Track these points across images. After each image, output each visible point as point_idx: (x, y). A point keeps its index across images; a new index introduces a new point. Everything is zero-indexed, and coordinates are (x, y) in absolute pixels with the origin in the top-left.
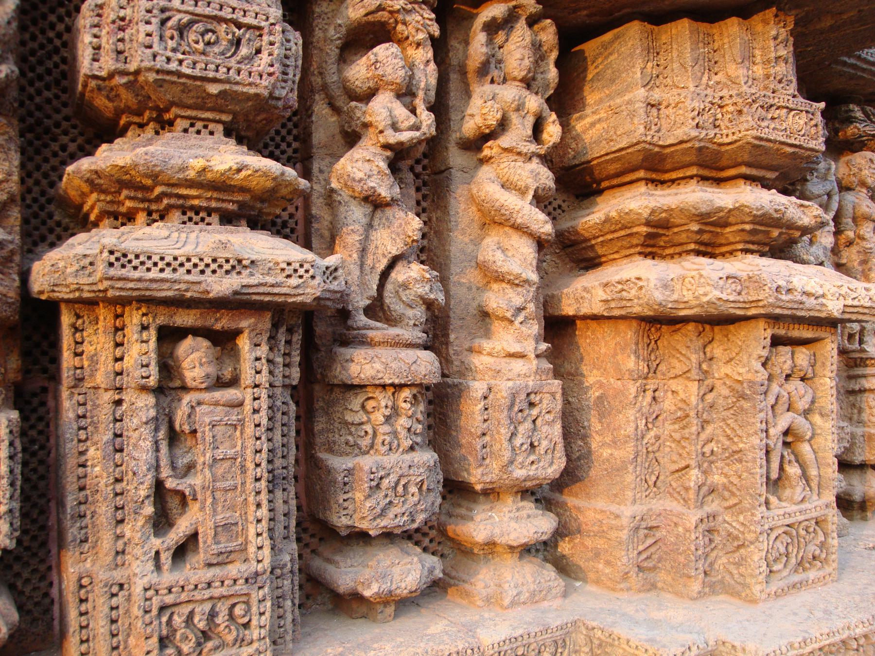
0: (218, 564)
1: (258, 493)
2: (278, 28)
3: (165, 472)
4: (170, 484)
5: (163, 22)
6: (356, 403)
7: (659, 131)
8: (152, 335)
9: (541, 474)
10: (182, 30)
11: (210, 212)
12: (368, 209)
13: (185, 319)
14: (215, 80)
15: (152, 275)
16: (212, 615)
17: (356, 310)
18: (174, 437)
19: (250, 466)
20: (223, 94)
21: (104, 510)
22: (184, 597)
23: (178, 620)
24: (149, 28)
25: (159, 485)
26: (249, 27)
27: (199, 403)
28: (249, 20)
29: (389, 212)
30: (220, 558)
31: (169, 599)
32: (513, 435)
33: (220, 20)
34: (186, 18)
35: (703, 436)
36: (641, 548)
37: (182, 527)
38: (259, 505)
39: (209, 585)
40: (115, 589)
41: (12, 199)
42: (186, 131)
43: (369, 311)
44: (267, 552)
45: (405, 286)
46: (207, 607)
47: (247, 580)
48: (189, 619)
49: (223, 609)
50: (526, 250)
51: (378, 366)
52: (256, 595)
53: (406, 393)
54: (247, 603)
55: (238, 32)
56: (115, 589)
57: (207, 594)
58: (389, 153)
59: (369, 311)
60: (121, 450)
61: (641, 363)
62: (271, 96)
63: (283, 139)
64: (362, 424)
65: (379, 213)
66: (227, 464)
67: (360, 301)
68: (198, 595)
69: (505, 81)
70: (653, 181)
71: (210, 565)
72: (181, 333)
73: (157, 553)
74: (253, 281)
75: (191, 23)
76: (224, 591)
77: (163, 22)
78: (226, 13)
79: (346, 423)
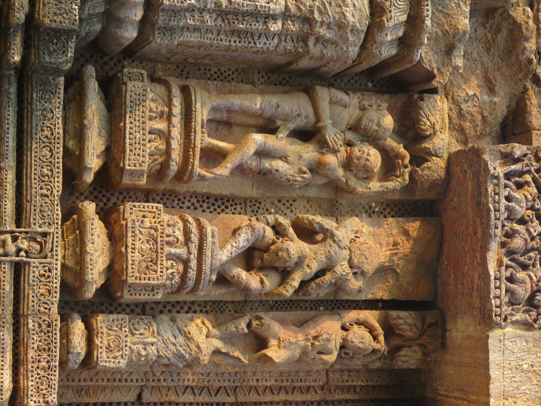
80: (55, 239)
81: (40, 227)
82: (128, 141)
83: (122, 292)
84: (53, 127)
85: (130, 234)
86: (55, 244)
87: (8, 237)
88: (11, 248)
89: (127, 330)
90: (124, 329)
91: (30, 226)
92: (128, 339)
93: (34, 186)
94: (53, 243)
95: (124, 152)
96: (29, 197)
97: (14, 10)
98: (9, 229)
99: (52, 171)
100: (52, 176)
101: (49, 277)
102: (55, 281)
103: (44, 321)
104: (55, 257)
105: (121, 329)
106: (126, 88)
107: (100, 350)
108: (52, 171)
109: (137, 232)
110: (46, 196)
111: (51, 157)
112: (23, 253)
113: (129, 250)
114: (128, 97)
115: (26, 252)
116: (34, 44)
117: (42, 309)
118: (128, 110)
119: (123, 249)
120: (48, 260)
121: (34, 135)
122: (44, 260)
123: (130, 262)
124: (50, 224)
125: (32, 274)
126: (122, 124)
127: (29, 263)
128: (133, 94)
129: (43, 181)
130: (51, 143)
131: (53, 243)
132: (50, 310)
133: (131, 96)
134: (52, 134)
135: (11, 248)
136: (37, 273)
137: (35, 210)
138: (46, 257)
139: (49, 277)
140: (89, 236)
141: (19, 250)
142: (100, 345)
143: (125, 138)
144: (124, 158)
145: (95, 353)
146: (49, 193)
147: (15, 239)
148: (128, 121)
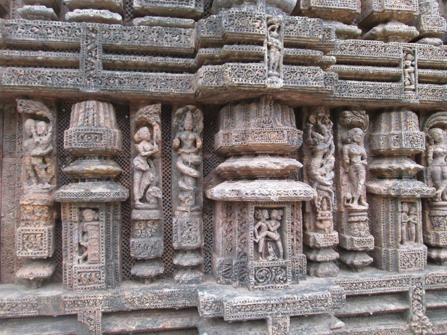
0: (92, 263)
1: (102, 247)
2: (106, 133)
3: (81, 241)
4: (81, 244)
5: (78, 136)
6: (137, 224)
7: (228, 142)
8: (77, 210)
9: (192, 245)
10: (82, 138)
11: (94, 179)
12: (141, 173)
13: (83, 206)
14: (90, 148)
15: (71, 197)
16: (90, 275)
17: (136, 199)
18: (84, 233)
19: (101, 240)
20: (93, 151)
21: (69, 250)
22: (84, 270)
23: (82, 276)
24: (74, 138)
25: (79, 244)
26: (99, 134)
27: (88, 225)
28: (99, 132)
29: (147, 173)
30: (93, 262)
31: (80, 270)
32: (182, 234)
33: (91, 133)
34: (83, 134)
35: (241, 237)
36: (224, 270)
37: (85, 254)
38: (103, 250)
39: (90, 268)
40: (70, 267)
41: (54, 177)
42: (88, 159)
43: (141, 200)
44: (104, 261)
45: (149, 193)
46: (89, 274)
47: (99, 268)
48: (85, 275)
49: (93, 274)
50: (190, 181)
51: (139, 215)
52: (101, 272)
53: (149, 222)
54: (100, 273)
55: (96, 135)
56: (70, 267)
57: (89, 270)
58: (145, 158)
59: (141, 200)
60: (72, 235)
61: (224, 214)
62: (106, 149)
63: (126, 152)
64: (138, 230)
65: (144, 173)
66: (95, 240)
67: (137, 197)
68: (87, 270)
69: (185, 130)
70: (236, 155)
71: (90, 263)
72: (85, 209)
73: (79, 260)
74: (94, 197)
75: (84, 135)
76: (93, 270)
77: (78, 136)
78: (93, 132)
79: (136, 230)
80: (406, 46)
81: (400, 53)
82: (343, 8)
83: (415, 16)
84: (350, 44)
85: (393, 8)
86: (408, 46)
87: (407, 70)
88: (411, 69)
89: (428, 16)
90: (428, 17)
91: (401, 59)
92: (433, 15)
93: (381, 56)
94: (408, 47)
95: (348, 10)
96: (385, 59)
97: (315, 56)
98: (402, 70)
99: (372, 46)
100: (374, 46)
101: (424, 50)
102: (425, 47)
103: (444, 53)
104: (415, 46)
105: (428, 19)
106: (313, 7)
107: (439, 30)
108: (372, 46)
109: (392, 4)
110: (385, 49)
111: (364, 46)
112: (413, 63)
113: (401, 9)
114: (320, 6)
115: (412, 61)
116: (324, 48)
117: (439, 54)
118: (326, 7)
119: (399, 13)
120: (416, 50)
121: (355, 55)
122: (416, 52)
123: (406, 9)
124: (398, 48)
125: (423, 59)
126: (333, 11)
127: (418, 60)
128: (317, 3)
129: (378, 51)
130: (358, 46)
131: (408, 47)
132: (439, 50)
133: (319, 4)
134: (353, 45)
135: (411, 69)
136: (423, 56)
137: (393, 56)
138: (414, 51)
139: (424, 50)
140: (395, 30)
141: (412, 65)
142: (436, 30)
143: (341, 9)
144: (351, 10)
145: (440, 32)
146: (384, 48)
147: (406, 67)
148: (333, 7)
